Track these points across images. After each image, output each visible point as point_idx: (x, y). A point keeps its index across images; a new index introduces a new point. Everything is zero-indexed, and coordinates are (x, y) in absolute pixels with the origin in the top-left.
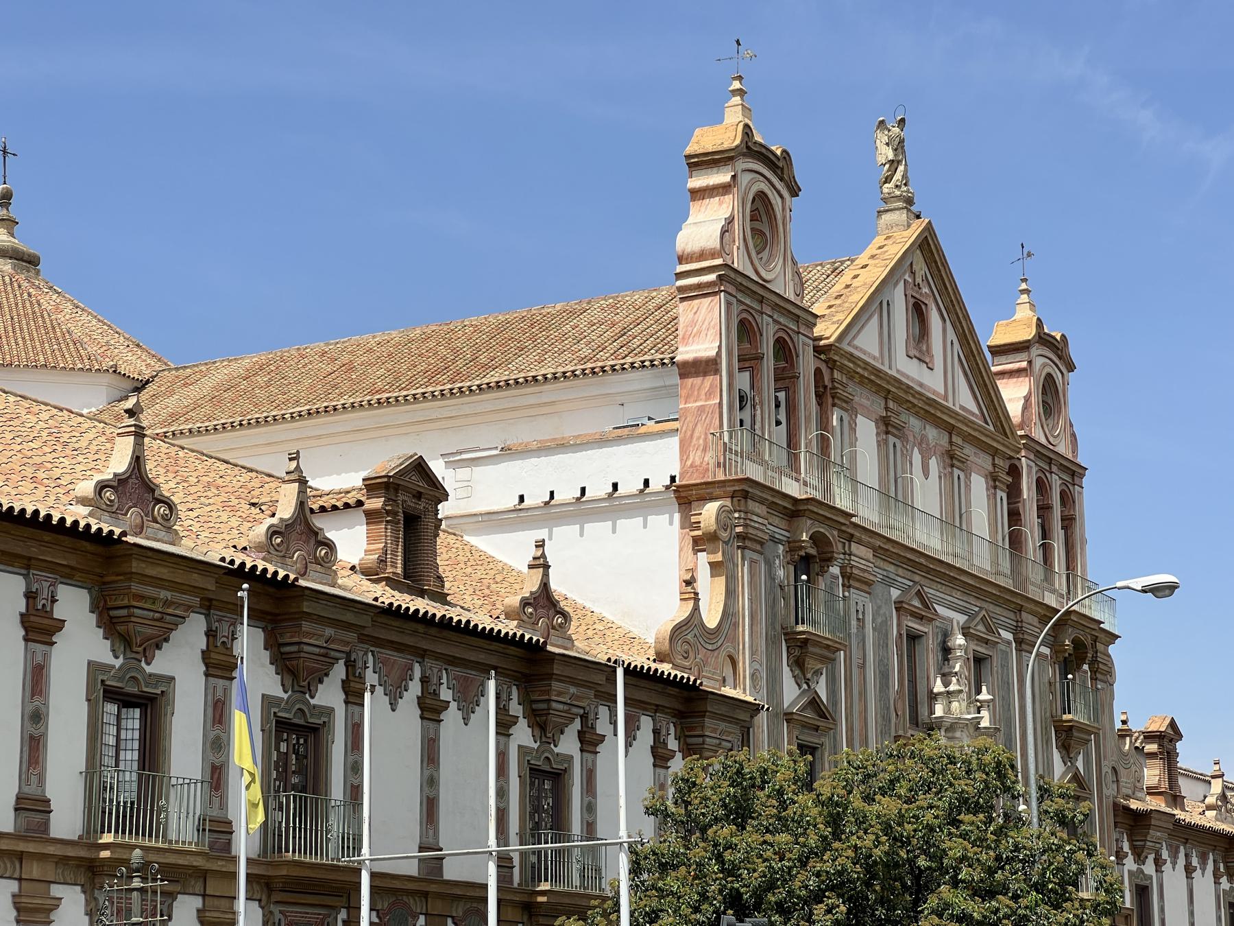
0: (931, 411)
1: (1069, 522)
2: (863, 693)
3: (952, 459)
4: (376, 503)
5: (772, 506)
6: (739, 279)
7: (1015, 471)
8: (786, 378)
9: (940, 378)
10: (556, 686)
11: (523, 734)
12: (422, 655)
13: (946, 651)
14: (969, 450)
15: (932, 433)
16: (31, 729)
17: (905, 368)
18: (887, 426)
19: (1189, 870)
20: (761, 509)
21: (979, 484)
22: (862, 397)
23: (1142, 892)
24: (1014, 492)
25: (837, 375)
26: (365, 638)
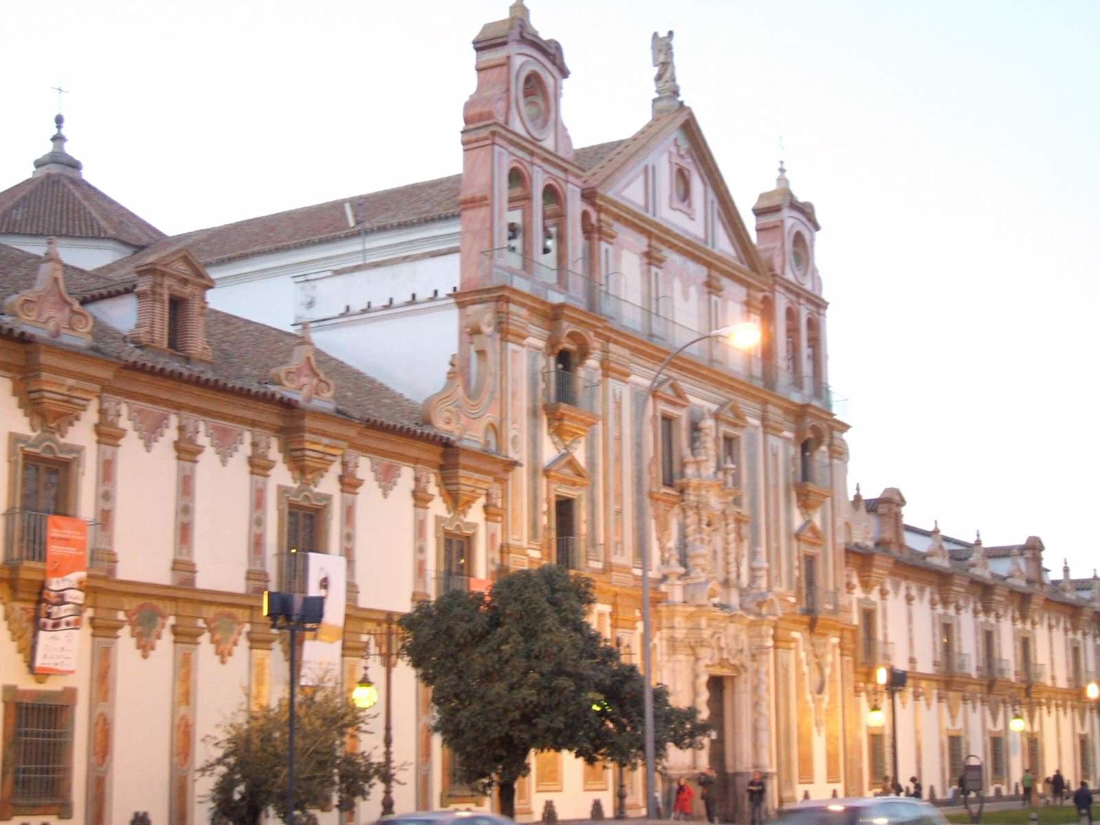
0: (693, 252)
1: (815, 341)
2: (619, 459)
3: (711, 287)
5: (532, 310)
6: (511, 136)
9: (691, 223)
10: (308, 436)
11: (438, 507)
12: (179, 407)
13: (695, 428)
15: (693, 268)
16: (182, 518)
17: (669, 215)
18: (651, 258)
19: (909, 599)
20: (524, 312)
22: (625, 235)
23: (868, 616)
25: (603, 216)
26: (353, 446)
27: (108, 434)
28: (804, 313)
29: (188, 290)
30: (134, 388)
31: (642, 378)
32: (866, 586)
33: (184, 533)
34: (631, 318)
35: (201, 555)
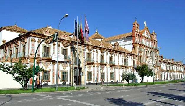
0: (147, 38)
8: (139, 37)
14: (150, 40)
18: (145, 39)
21: (151, 42)
23: (161, 65)
27: (114, 55)
31: (145, 48)
32: (161, 63)
34: (144, 44)
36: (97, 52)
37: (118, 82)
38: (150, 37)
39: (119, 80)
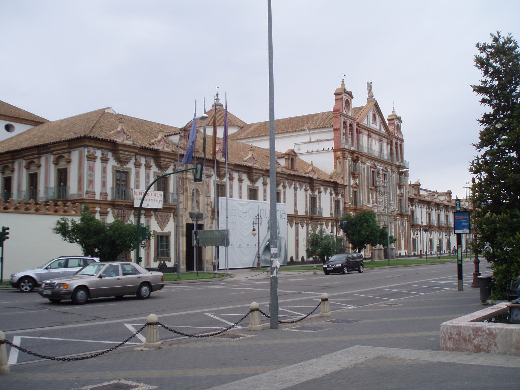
1: (401, 149)
2: (364, 182)
3: (380, 140)
4: (286, 157)
5: (349, 152)
7: (391, 142)
9: (376, 126)
12: (294, 180)
13: (378, 173)
18: (369, 136)
20: (347, 153)
21: (385, 145)
22: (363, 131)
24: (391, 145)
27: (284, 187)
28: (399, 143)
29: (293, 157)
30: (295, 179)
31: (369, 164)
33: (296, 204)
34: (365, 150)
35: (298, 209)
36: (240, 180)
37: (294, 260)
38: (383, 130)
39: (297, 257)
